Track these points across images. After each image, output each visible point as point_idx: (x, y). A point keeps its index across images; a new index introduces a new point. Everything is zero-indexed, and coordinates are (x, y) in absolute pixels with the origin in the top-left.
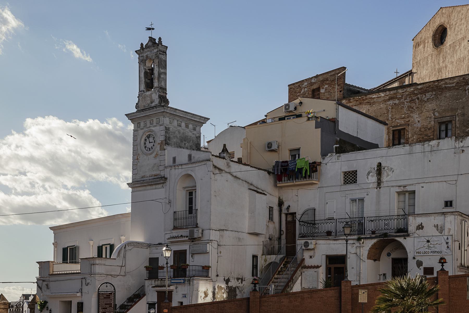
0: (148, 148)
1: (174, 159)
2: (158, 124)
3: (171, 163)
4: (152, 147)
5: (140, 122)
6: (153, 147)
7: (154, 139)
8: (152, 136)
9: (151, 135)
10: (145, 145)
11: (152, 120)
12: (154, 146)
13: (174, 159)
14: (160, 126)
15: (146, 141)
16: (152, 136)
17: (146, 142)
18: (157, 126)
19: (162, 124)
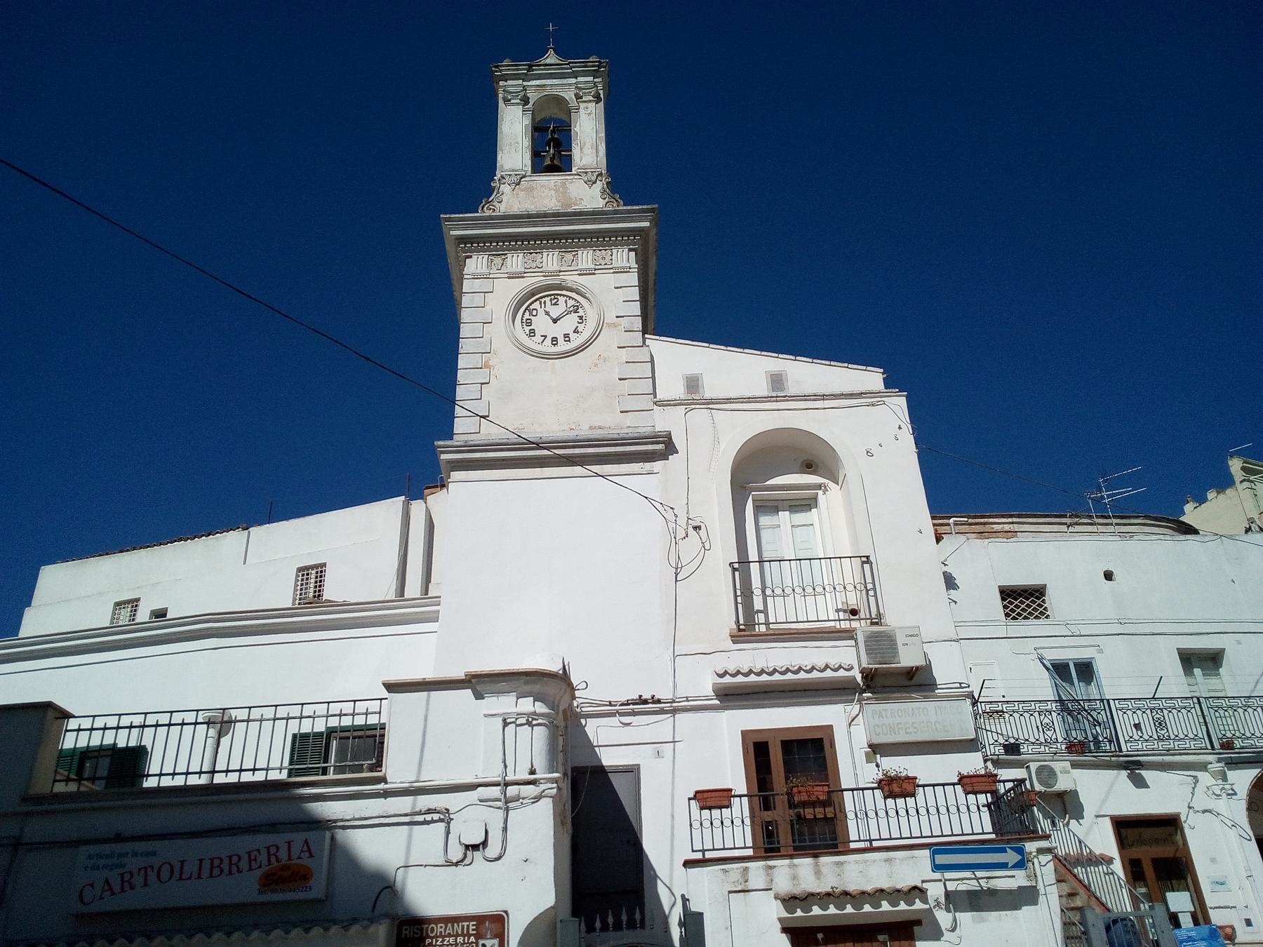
0: (545, 336)
1: (693, 383)
2: (606, 267)
3: (679, 391)
4: (566, 336)
5: (506, 254)
6: (573, 336)
7: (580, 310)
8: (566, 302)
9: (562, 299)
10: (527, 329)
11: (574, 253)
12: (576, 331)
13: (693, 383)
14: (614, 273)
15: (531, 314)
16: (566, 302)
17: (531, 317)
18: (596, 272)
19: (623, 268)
